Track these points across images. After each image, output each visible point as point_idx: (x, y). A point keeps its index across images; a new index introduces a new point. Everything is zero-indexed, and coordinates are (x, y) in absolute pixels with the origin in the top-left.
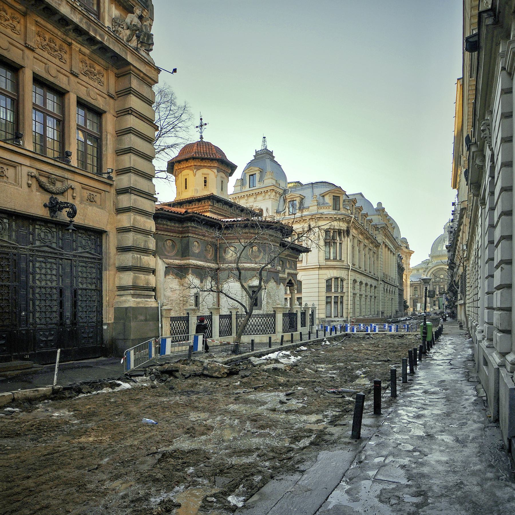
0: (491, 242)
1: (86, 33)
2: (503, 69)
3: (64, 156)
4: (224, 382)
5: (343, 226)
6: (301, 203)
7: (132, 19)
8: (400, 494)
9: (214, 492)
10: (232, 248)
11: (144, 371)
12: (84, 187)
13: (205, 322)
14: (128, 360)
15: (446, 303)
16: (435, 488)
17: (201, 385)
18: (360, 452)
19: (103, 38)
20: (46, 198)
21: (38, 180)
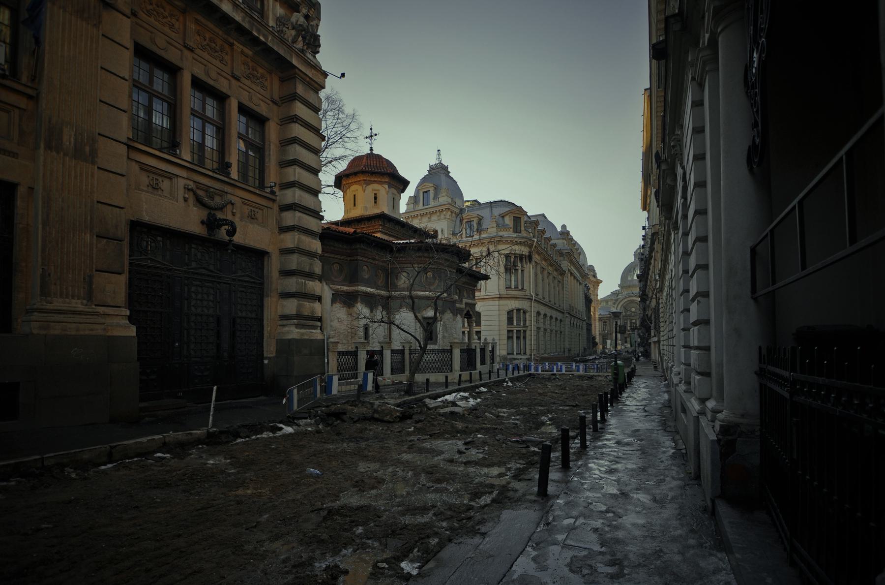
0: (686, 272)
1: (250, 33)
2: (693, 79)
3: (224, 167)
4: (397, 427)
5: (525, 251)
6: (479, 224)
7: (297, 18)
8: (593, 563)
10: (405, 274)
11: (307, 413)
12: (245, 202)
13: (376, 357)
14: (290, 400)
15: (639, 340)
16: (631, 556)
17: (370, 430)
18: (548, 512)
19: (266, 38)
20: (204, 214)
21: (195, 193)
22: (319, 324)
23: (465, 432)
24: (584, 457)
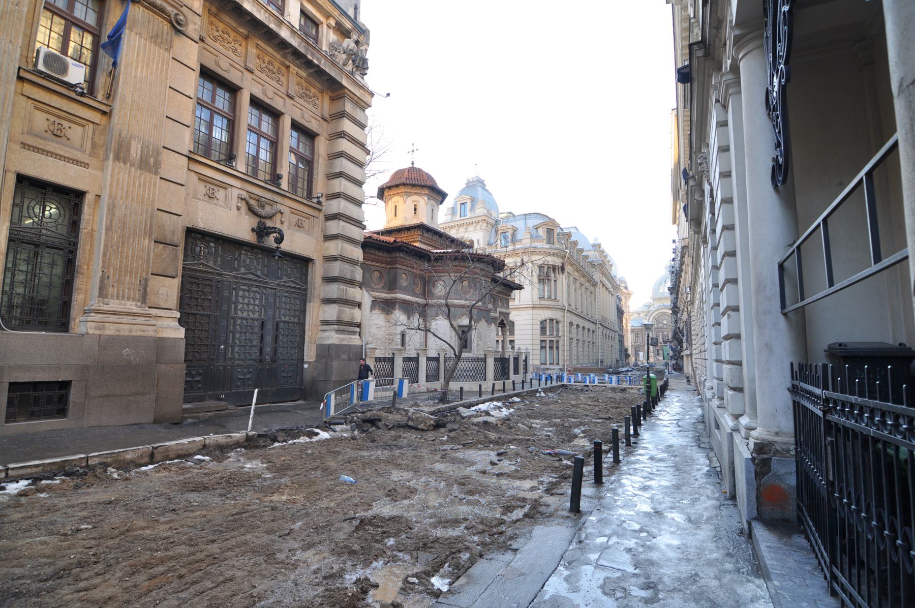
1: (304, 57)
3: (275, 178)
4: (430, 435)
9: (416, 570)
10: (441, 283)
21: (247, 203)
22: (358, 330)
23: (497, 442)
24: (617, 472)
